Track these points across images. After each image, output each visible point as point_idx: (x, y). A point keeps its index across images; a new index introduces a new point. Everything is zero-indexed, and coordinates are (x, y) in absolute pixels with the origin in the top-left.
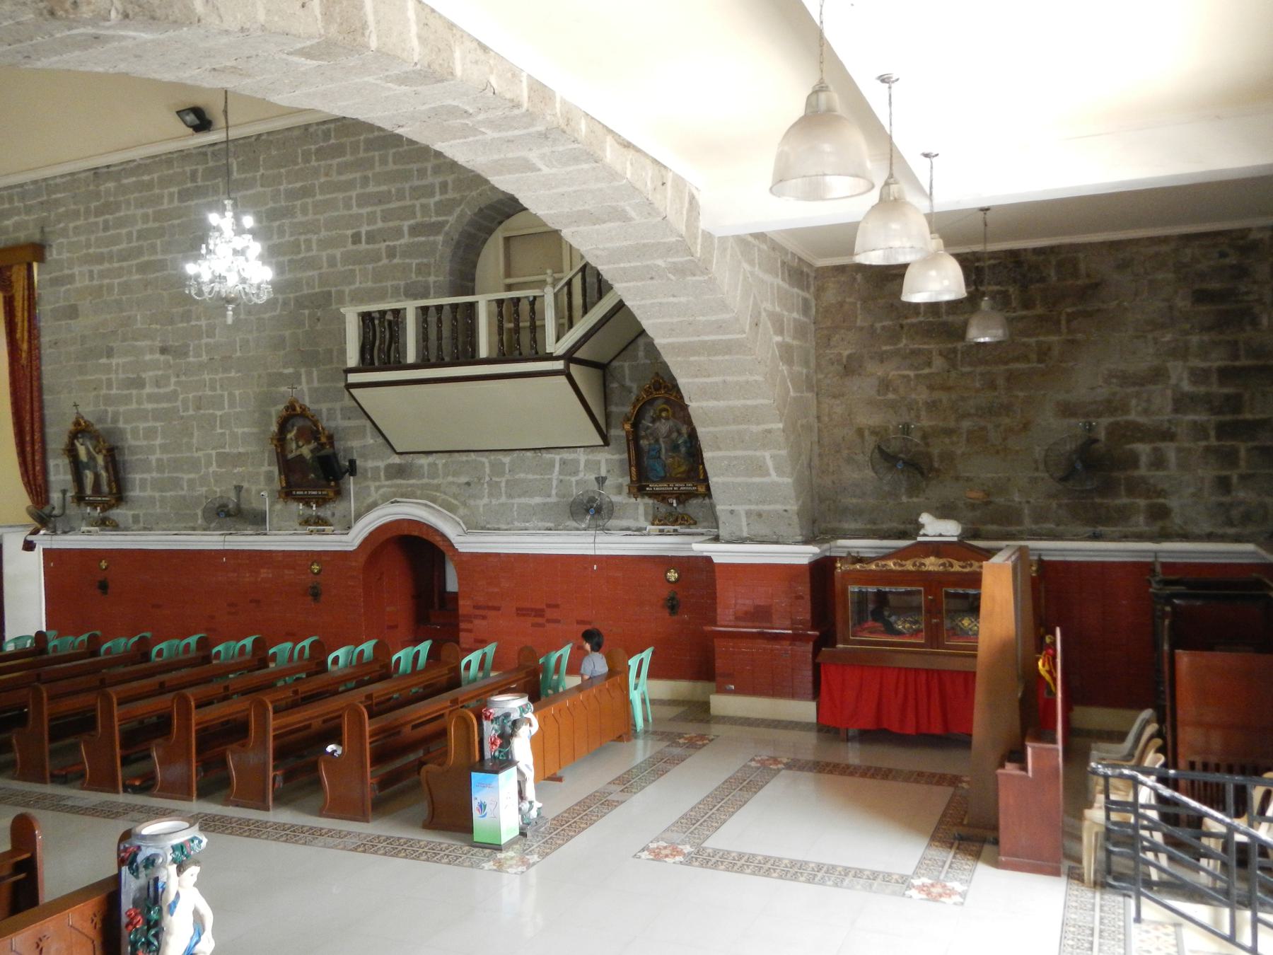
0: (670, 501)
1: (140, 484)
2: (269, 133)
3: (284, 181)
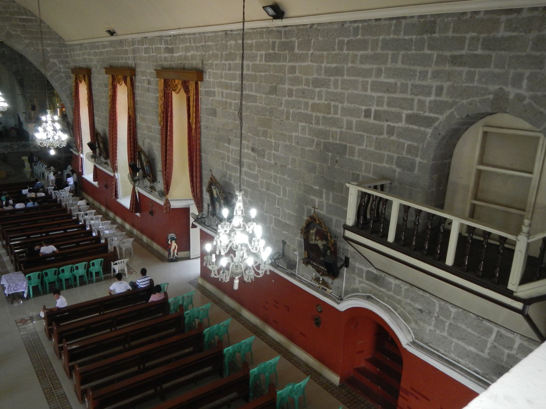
2: (319, 24)
3: (325, 61)
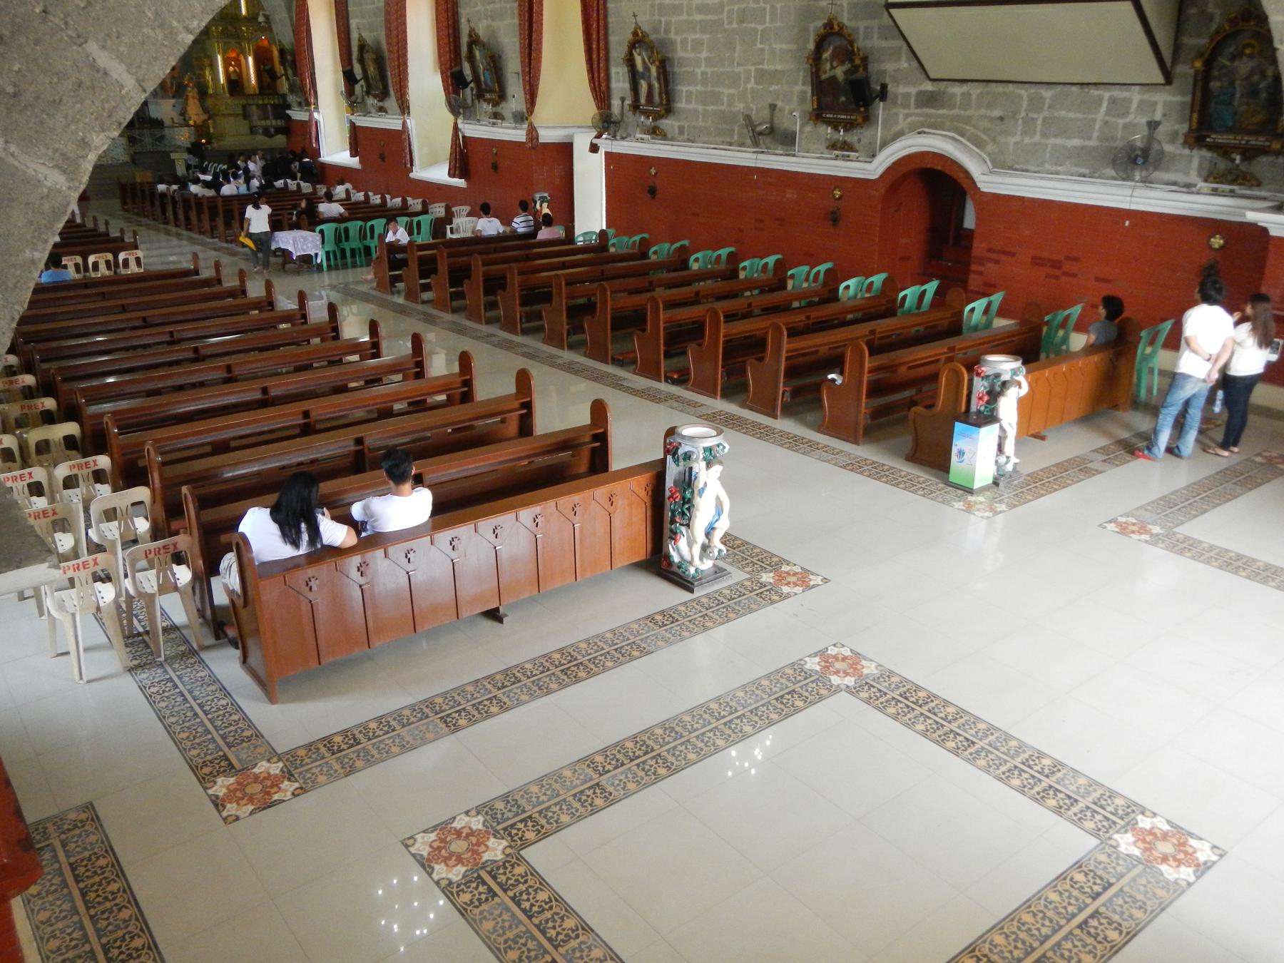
0: (1233, 156)
1: (687, 95)
